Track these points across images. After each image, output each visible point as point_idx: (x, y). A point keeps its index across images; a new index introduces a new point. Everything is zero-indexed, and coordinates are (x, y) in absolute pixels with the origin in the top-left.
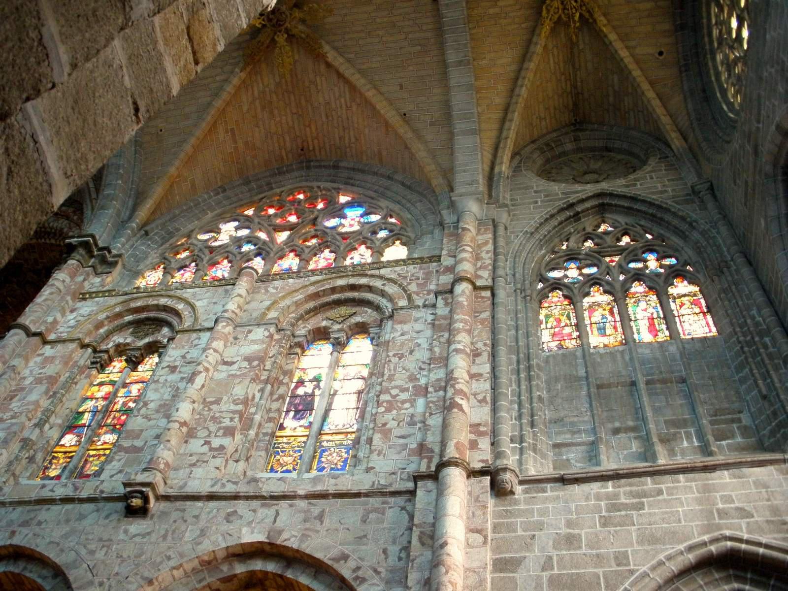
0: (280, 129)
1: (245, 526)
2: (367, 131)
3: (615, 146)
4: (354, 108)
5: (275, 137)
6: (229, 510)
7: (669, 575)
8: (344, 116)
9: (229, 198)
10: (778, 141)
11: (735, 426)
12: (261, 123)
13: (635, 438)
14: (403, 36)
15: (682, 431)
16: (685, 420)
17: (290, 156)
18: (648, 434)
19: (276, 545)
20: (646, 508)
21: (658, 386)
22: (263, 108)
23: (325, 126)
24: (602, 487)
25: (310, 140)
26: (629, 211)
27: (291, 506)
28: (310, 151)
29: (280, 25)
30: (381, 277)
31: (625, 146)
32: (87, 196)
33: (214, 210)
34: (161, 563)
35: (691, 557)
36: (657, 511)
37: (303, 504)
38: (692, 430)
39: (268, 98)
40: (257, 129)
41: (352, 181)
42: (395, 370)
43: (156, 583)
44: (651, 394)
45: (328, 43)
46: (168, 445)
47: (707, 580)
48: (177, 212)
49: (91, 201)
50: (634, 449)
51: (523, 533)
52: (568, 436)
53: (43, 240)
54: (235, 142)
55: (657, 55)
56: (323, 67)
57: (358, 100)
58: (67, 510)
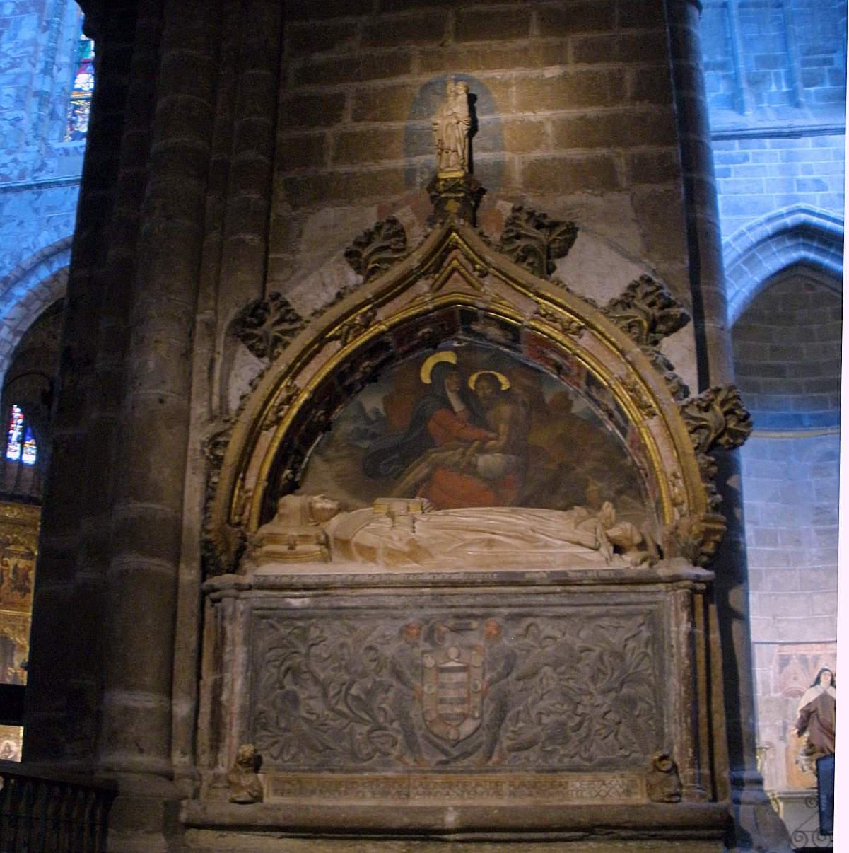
7: (748, 245)
11: (826, 68)
13: (724, 77)
15: (773, 71)
16: (776, 58)
18: (737, 74)
20: (733, 174)
21: (752, 10)
35: (769, 229)
36: (741, 178)
38: (782, 71)
44: (743, 21)
47: (780, 247)
50: (721, 91)
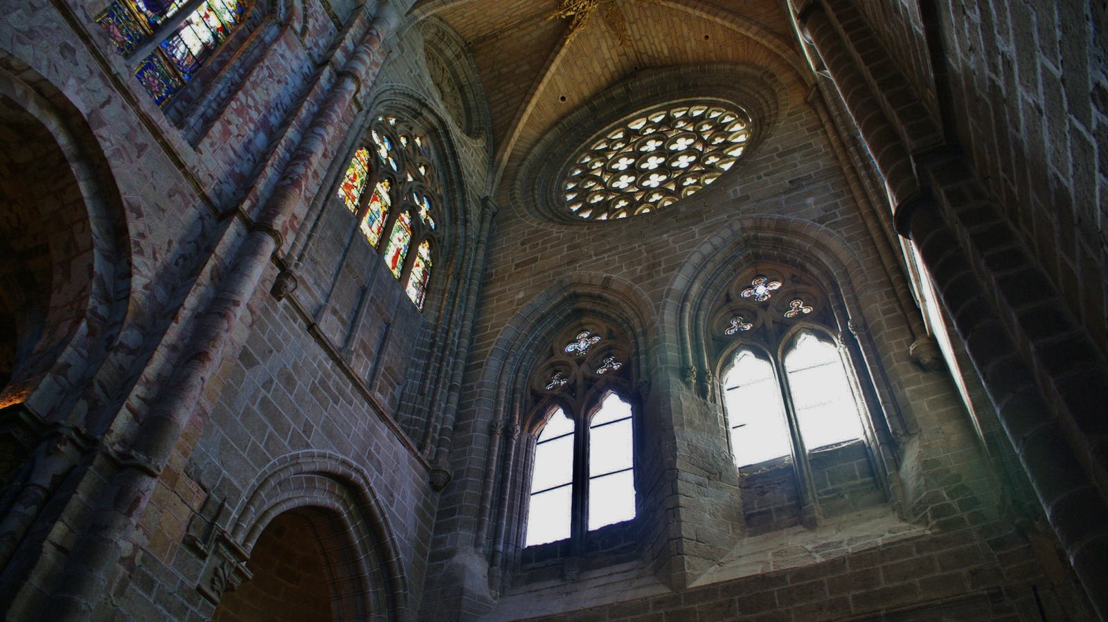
3: (468, 95)
6: (68, 41)
10: (594, 282)
19: (91, 132)
24: (326, 359)
26: (442, 157)
27: (124, 107)
31: (472, 103)
37: (134, 118)
42: (261, 82)
51: (267, 340)
52: (312, 281)
55: (561, 96)
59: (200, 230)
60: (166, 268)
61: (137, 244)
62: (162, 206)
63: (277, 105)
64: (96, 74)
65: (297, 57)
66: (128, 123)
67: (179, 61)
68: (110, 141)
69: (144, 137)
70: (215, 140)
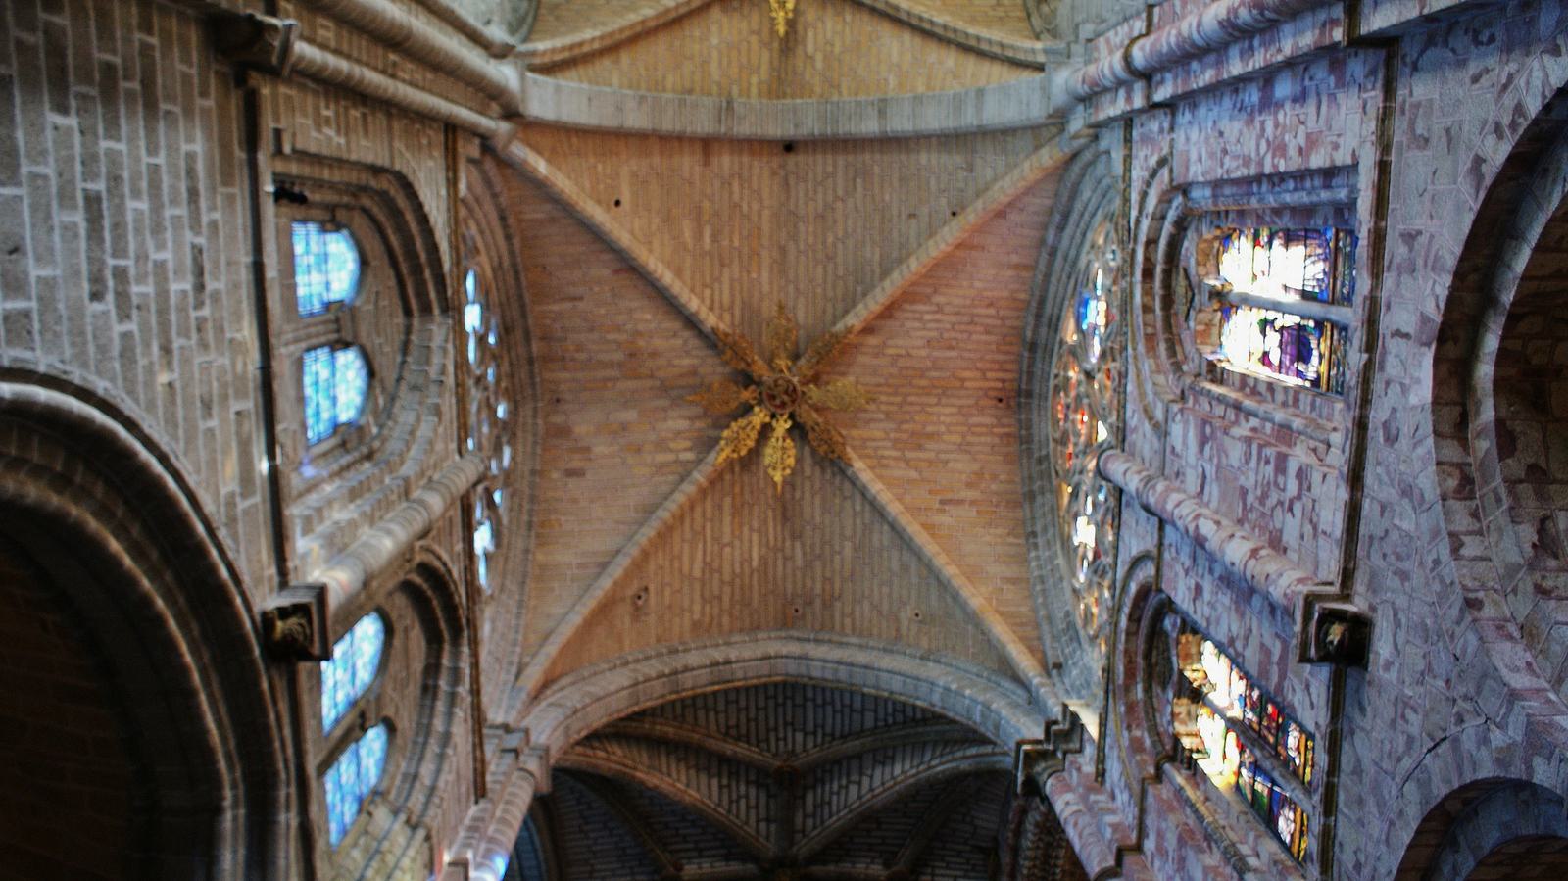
0: (959, 429)
1: (1407, 398)
2: (978, 284)
4: (939, 299)
5: (970, 438)
6: (1381, 439)
8: (954, 319)
9: (1045, 530)
12: (943, 456)
14: (839, 204)
17: (1005, 421)
19: (1442, 324)
22: (920, 447)
23: (966, 354)
25: (987, 385)
27: (1388, 307)
28: (1003, 389)
29: (794, 390)
30: (1138, 221)
32: (987, 759)
33: (1056, 553)
34: (1442, 581)
37: (1389, 280)
39: (905, 436)
40: (950, 465)
41: (1054, 320)
43: (1481, 595)
45: (834, 324)
46: (1273, 577)
48: (1042, 613)
49: (993, 754)
53: (1058, 871)
54: (960, 502)
56: (872, 341)
57: (929, 290)
58: (1346, 804)
59: (1428, 52)
60: (1508, 49)
61: (1513, 126)
62: (1444, 140)
63: (1240, 110)
64: (1385, 376)
65: (1188, 139)
66: (1398, 285)
67: (1325, 260)
68: (1432, 289)
69: (1395, 249)
70: (1329, 148)
